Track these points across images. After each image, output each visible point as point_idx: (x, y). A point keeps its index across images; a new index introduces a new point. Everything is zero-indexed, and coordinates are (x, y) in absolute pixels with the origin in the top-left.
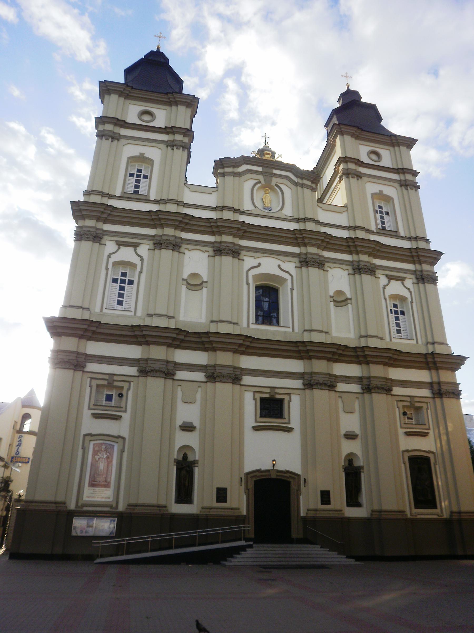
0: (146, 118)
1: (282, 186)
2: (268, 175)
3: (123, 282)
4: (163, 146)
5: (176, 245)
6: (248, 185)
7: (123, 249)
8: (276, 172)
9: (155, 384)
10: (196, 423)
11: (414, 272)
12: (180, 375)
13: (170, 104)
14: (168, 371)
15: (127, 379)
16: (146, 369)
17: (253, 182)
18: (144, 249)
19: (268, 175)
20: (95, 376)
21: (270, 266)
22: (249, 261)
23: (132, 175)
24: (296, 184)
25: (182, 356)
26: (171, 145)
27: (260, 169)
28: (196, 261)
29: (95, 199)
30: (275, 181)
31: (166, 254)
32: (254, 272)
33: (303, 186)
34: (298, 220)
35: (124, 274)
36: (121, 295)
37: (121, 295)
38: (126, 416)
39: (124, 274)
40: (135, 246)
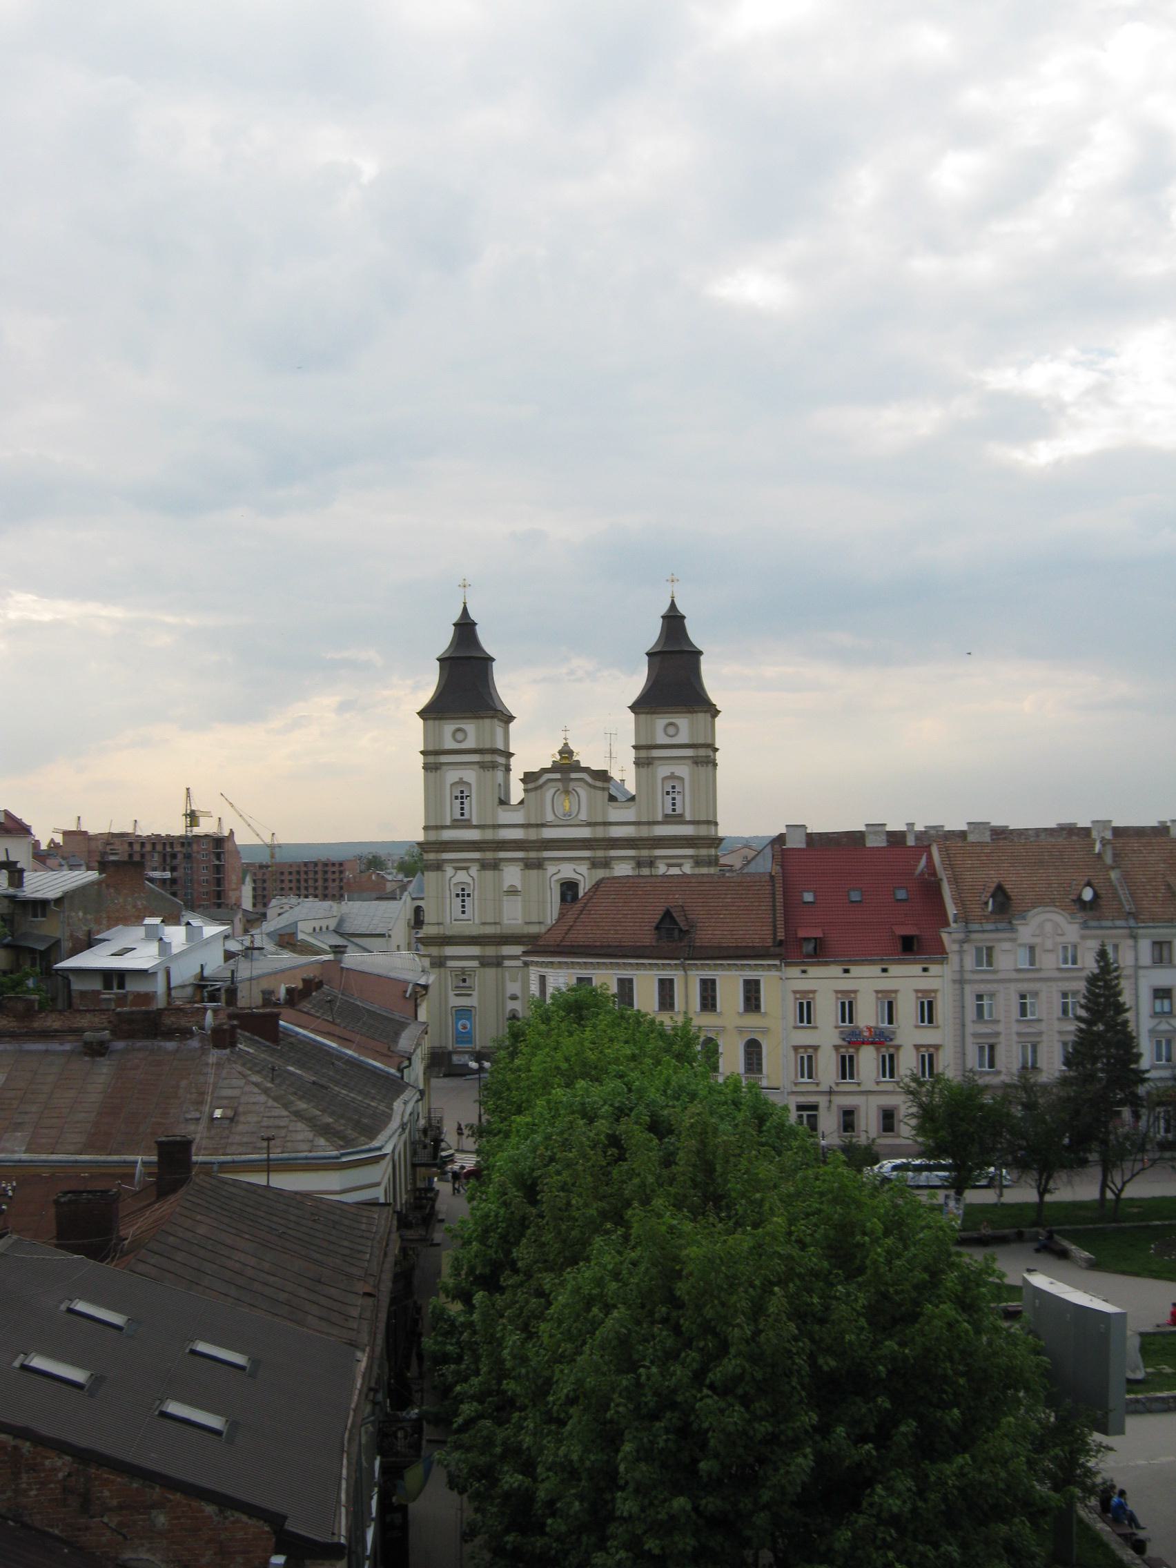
0: (460, 736)
1: (578, 789)
2: (566, 781)
3: (463, 895)
4: (476, 767)
5: (495, 866)
6: (549, 793)
7: (459, 872)
8: (573, 776)
9: (491, 972)
10: (519, 994)
11: (691, 857)
12: (507, 963)
13: (477, 716)
14: (498, 962)
15: (473, 969)
16: (485, 962)
17: (552, 791)
18: (474, 870)
19: (566, 781)
20: (453, 969)
21: (568, 871)
22: (551, 869)
23: (456, 798)
24: (590, 785)
25: (507, 950)
26: (482, 766)
27: (558, 776)
28: (512, 875)
29: (433, 836)
30: (572, 785)
31: (489, 874)
32: (556, 877)
33: (595, 787)
34: (589, 824)
35: (463, 890)
36: (463, 906)
37: (463, 906)
38: (475, 993)
39: (463, 890)
40: (467, 869)
